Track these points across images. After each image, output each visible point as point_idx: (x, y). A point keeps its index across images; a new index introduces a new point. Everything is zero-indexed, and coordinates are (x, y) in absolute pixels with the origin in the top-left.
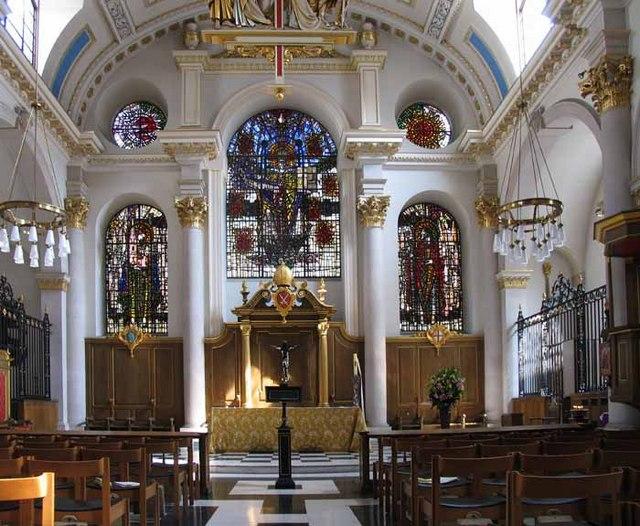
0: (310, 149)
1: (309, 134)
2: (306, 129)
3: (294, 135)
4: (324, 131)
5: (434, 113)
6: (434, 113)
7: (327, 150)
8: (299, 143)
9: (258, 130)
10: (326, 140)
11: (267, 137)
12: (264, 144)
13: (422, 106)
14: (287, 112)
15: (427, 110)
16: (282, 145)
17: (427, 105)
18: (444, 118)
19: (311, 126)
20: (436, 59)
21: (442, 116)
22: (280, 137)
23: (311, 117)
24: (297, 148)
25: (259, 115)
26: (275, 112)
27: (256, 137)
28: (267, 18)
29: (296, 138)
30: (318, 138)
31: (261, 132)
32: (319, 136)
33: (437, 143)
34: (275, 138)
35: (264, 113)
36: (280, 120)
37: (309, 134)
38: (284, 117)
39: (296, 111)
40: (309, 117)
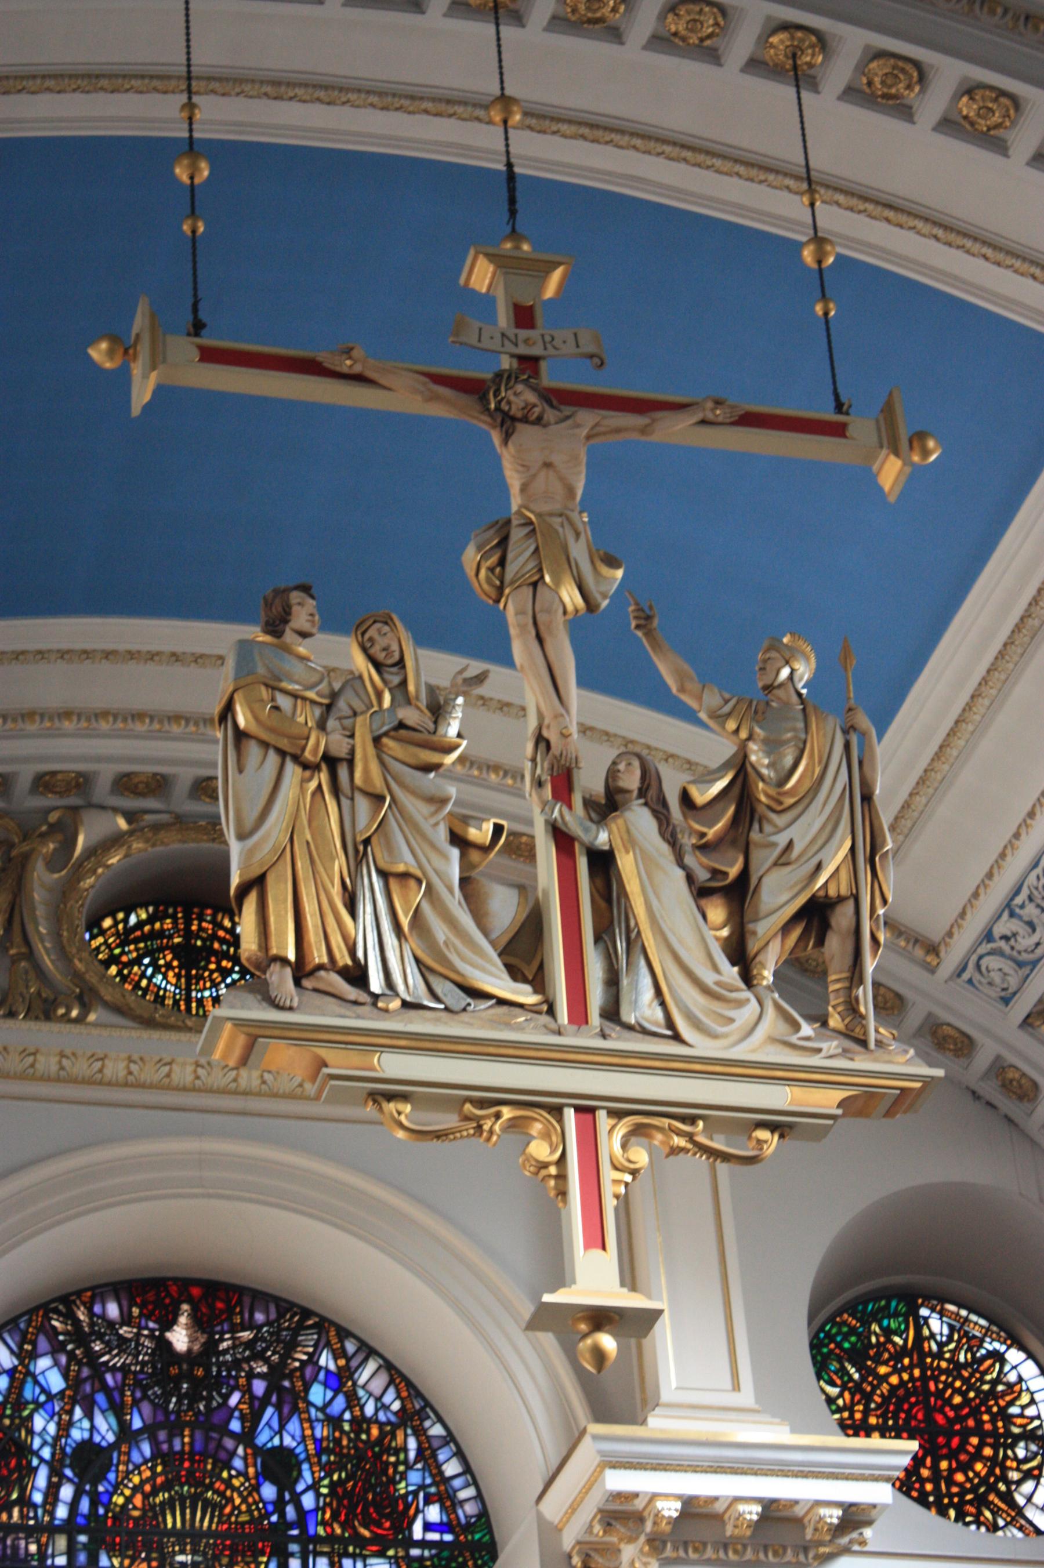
0: (344, 1502)
1: (335, 1422)
2: (317, 1394)
3: (252, 1420)
4: (417, 1407)
5: (973, 1343)
6: (973, 1343)
7: (434, 1513)
8: (280, 1466)
9: (56, 1382)
10: (427, 1455)
11: (105, 1429)
12: (88, 1462)
13: (910, 1300)
14: (217, 1299)
15: (936, 1324)
16: (189, 1472)
17: (938, 1299)
18: (1029, 1369)
19: (340, 1381)
20: (990, 1090)
21: (1014, 1356)
22: (175, 1429)
23: (344, 1333)
24: (269, 1491)
25: (64, 1302)
26: (154, 1293)
27: (39, 1422)
28: (515, 973)
29: (263, 1438)
30: (384, 1445)
31: (76, 1397)
32: (388, 1431)
33: (1008, 1498)
34: (150, 1430)
35: (98, 1292)
36: (180, 1338)
37: (335, 1422)
38: (198, 1323)
39: (260, 1297)
40: (331, 1330)
